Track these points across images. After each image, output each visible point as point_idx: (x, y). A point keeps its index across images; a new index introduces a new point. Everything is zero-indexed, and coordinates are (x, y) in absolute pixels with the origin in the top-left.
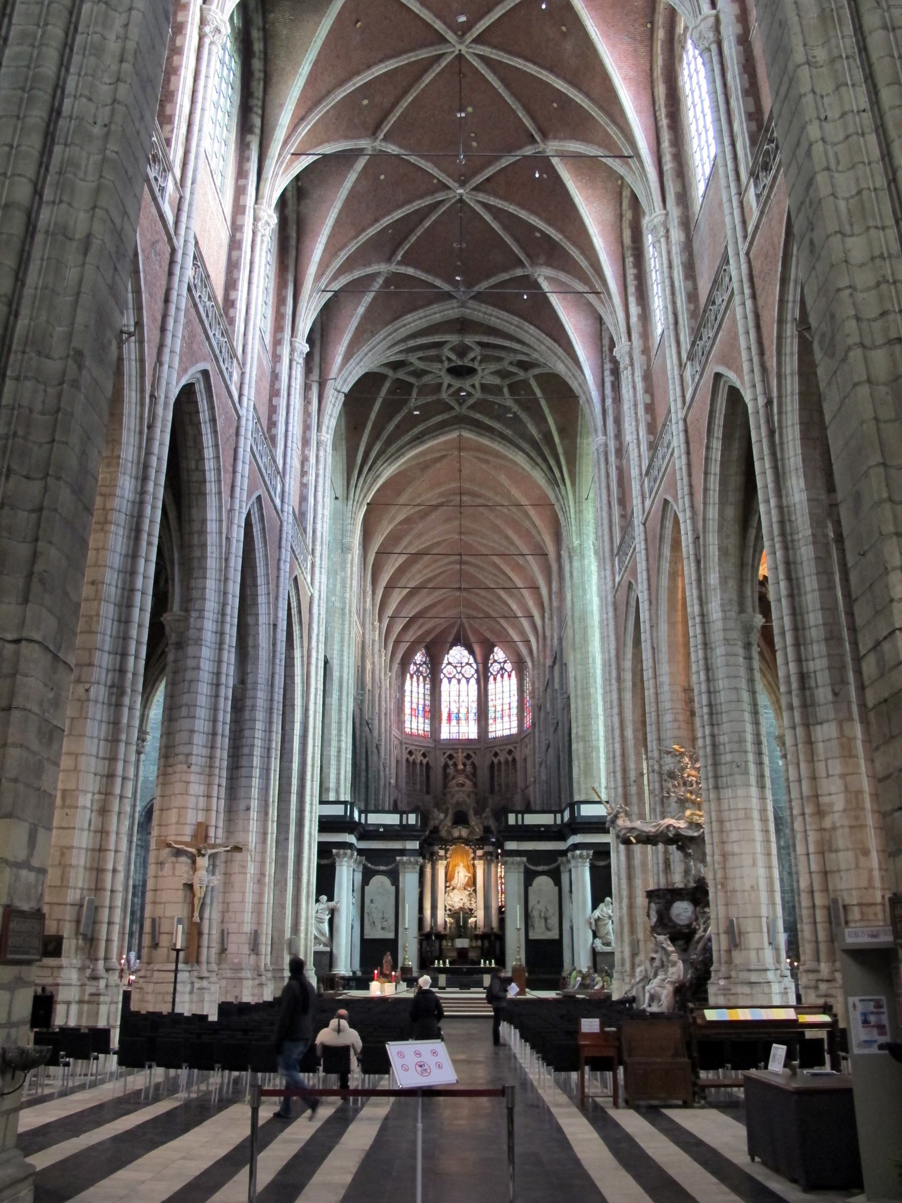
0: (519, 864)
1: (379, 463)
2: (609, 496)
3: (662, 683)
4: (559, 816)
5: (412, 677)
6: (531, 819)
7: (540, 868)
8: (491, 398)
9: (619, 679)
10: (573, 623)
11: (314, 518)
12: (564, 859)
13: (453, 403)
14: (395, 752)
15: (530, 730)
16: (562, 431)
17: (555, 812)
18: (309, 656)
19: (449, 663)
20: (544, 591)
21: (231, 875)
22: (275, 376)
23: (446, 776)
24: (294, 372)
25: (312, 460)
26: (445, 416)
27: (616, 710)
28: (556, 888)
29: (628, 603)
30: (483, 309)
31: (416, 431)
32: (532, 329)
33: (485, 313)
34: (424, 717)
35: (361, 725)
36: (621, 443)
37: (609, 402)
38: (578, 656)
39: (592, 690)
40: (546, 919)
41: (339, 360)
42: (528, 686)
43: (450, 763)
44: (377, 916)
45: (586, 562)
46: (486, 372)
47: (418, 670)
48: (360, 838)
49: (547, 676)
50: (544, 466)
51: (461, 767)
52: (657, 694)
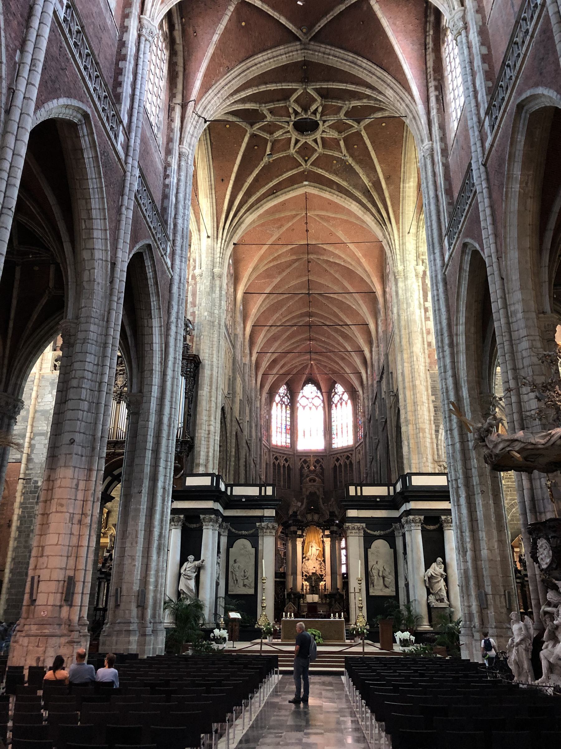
0: (359, 529)
1: (243, 211)
2: (436, 190)
3: (515, 313)
4: (391, 488)
5: (277, 404)
6: (369, 491)
7: (377, 533)
8: (330, 153)
9: (451, 345)
10: (400, 331)
11: (175, 215)
12: (398, 525)
13: (300, 160)
14: (265, 458)
15: (362, 440)
16: (387, 179)
17: (388, 485)
18: (168, 329)
19: (303, 396)
20: (372, 327)
21: (48, 515)
22: (122, 44)
23: (301, 475)
24: (142, 46)
25: (174, 166)
26: (294, 172)
27: (450, 373)
28: (392, 550)
29: (461, 269)
30: (322, 50)
31: (271, 185)
32: (365, 63)
33: (324, 53)
34: (286, 433)
35: (231, 420)
36: (446, 145)
37: (434, 113)
38: (405, 356)
39: (417, 383)
40: (384, 578)
41: (198, 85)
42: (361, 409)
43: (305, 466)
44: (239, 575)
45: (409, 282)
46: (327, 124)
47: (281, 400)
48: (225, 508)
49: (375, 392)
50: (374, 210)
51: (312, 468)
52: (508, 324)
